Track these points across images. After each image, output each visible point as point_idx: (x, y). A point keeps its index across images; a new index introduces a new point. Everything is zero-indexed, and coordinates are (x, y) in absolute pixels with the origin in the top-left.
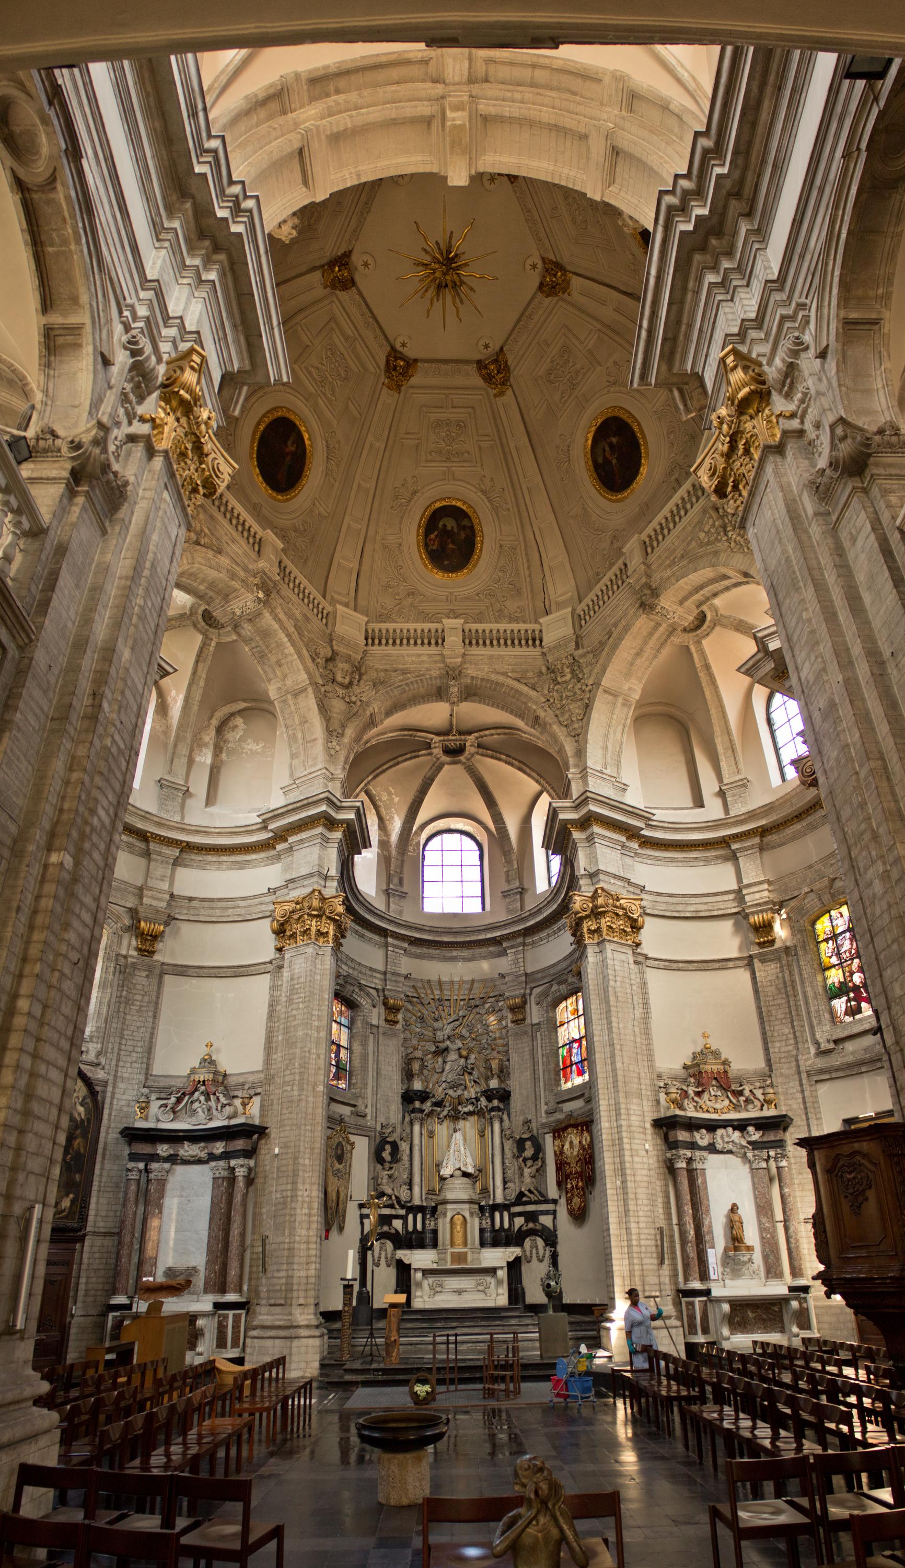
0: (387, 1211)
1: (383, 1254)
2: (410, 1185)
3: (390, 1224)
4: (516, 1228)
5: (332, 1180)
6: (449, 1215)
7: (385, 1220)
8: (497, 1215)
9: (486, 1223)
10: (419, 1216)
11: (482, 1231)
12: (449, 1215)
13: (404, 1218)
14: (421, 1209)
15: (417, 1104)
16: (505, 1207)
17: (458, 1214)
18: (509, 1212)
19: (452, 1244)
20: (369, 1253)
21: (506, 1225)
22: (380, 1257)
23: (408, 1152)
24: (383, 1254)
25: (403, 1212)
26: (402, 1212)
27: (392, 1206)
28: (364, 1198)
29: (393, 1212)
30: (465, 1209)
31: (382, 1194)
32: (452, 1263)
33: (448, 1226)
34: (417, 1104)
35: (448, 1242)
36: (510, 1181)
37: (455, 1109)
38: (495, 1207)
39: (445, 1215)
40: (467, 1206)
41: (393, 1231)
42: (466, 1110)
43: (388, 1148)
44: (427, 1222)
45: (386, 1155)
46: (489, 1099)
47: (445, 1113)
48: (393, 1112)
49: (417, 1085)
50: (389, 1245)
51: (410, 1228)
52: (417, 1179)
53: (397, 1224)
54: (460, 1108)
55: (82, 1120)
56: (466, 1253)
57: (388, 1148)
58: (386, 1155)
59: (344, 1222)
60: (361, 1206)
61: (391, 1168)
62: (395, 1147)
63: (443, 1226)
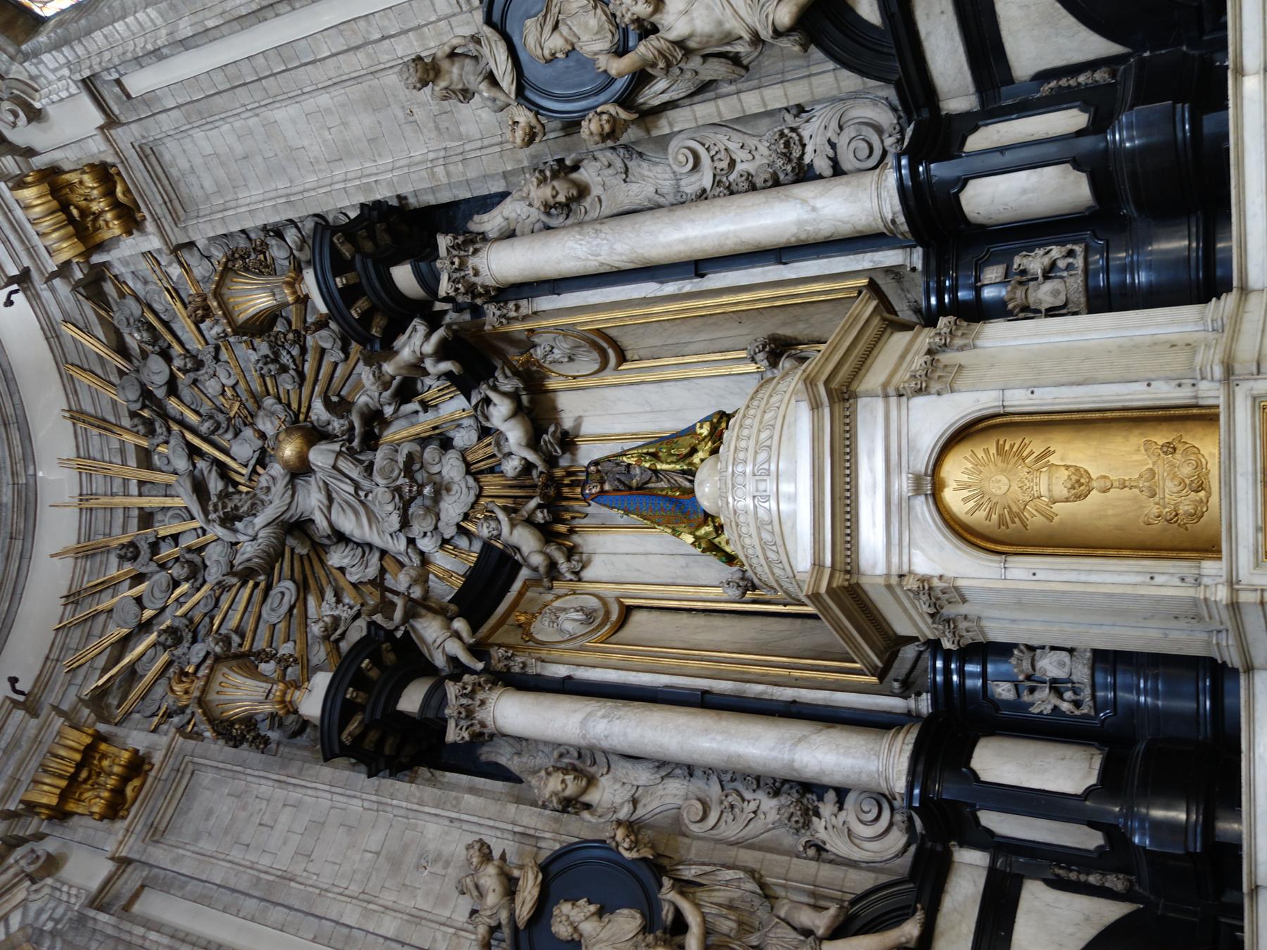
2: (806, 793)
4: (1093, 45)
6: (936, 557)
8: (989, 198)
9: (1054, 268)
10: (997, 763)
11: (1103, 299)
12: (936, 557)
14: (948, 734)
16: (932, 136)
17: (931, 484)
18: (971, 122)
19: (1194, 542)
21: (1069, 120)
23: (642, 776)
25: (969, 873)
26: (969, 873)
30: (901, 428)
33: (1023, 572)
35: (1165, 580)
36: (789, 144)
38: (934, 221)
39: (937, 597)
40: (871, 421)
42: (514, 435)
44: (1042, 703)
46: (402, 313)
47: (526, 541)
48: (441, 823)
51: (1088, 839)
52: (759, 745)
54: (511, 467)
63: (1054, 608)
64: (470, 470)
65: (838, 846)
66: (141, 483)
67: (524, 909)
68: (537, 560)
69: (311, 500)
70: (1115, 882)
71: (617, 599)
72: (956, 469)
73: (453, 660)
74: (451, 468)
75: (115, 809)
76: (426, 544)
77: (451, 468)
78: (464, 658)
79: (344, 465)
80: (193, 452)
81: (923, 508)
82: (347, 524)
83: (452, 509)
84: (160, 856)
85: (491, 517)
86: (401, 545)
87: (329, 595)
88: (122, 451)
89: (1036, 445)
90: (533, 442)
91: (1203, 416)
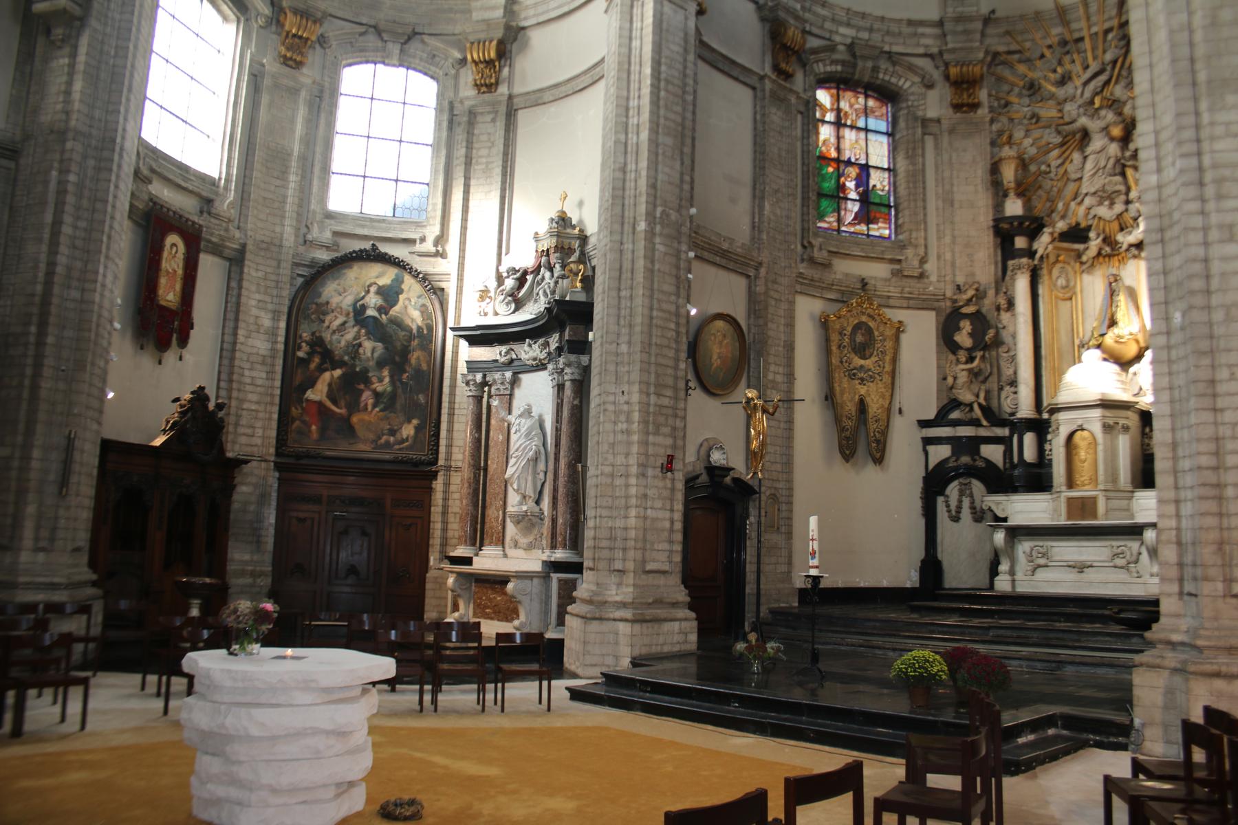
0: (965, 431)
1: (966, 502)
3: (977, 451)
5: (843, 384)
6: (1064, 431)
7: (973, 444)
13: (1005, 441)
15: (1020, 242)
19: (1071, 484)
20: (940, 500)
22: (959, 508)
24: (966, 502)
27: (976, 423)
28: (931, 415)
29: (983, 432)
31: (955, 404)
32: (1069, 517)
34: (1020, 242)
37: (1108, 241)
40: (1097, 413)
41: (981, 464)
43: (966, 326)
45: (963, 338)
48: (980, 262)
49: (1014, 207)
50: (977, 486)
53: (993, 453)
54: (1120, 237)
55: (419, 328)
56: (1094, 500)
57: (966, 326)
58: (963, 338)
59: (883, 451)
60: (924, 424)
61: (971, 359)
62: (980, 322)
64: (1119, 216)
65: (1003, 394)
66: (1096, 34)
67: (965, 310)
68: (1084, 258)
69: (1097, 143)
70: (1008, 465)
71: (1075, 293)
72: (1085, 433)
73: (1036, 252)
74: (1119, 208)
75: (957, 107)
76: (1087, 201)
77: (1119, 208)
78: (1038, 256)
79: (1112, 161)
80: (1115, 62)
81: (1074, 427)
82: (1089, 165)
83: (1103, 211)
84: (945, 139)
85: (1098, 235)
86: (1084, 191)
87: (1060, 161)
88: (1110, 19)
89: (1091, 451)
90: (1131, 245)
91: (1097, 484)
